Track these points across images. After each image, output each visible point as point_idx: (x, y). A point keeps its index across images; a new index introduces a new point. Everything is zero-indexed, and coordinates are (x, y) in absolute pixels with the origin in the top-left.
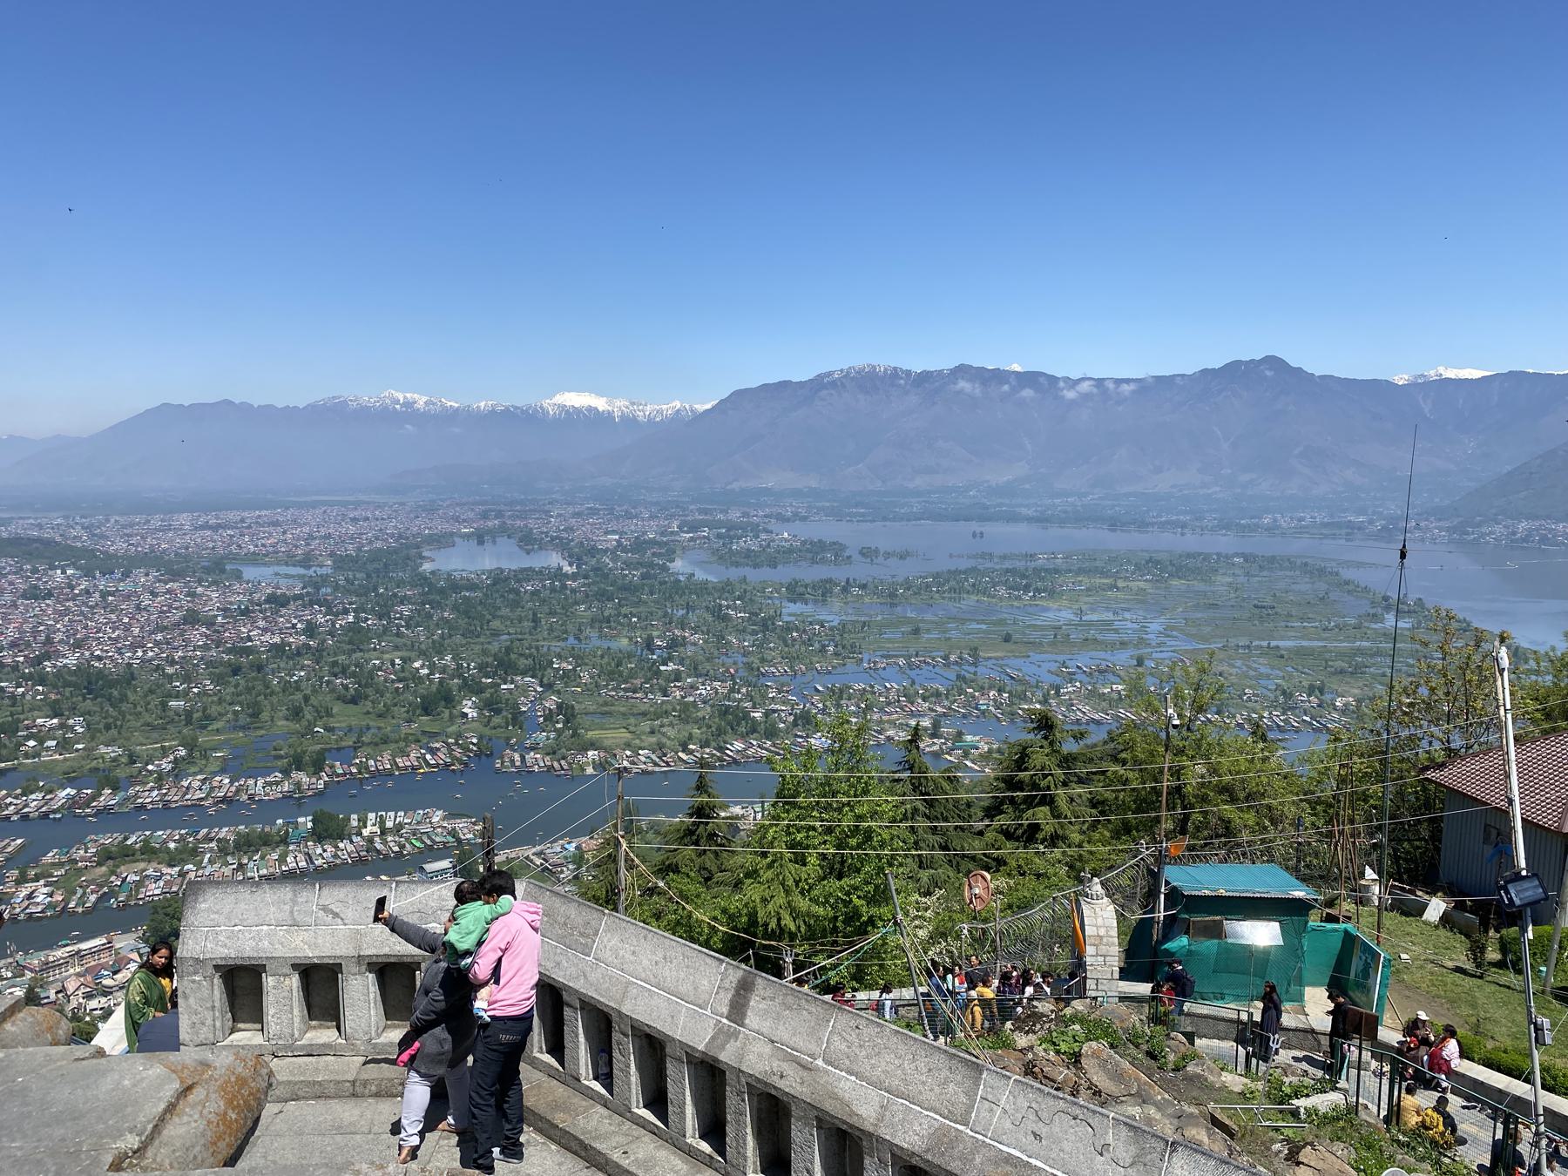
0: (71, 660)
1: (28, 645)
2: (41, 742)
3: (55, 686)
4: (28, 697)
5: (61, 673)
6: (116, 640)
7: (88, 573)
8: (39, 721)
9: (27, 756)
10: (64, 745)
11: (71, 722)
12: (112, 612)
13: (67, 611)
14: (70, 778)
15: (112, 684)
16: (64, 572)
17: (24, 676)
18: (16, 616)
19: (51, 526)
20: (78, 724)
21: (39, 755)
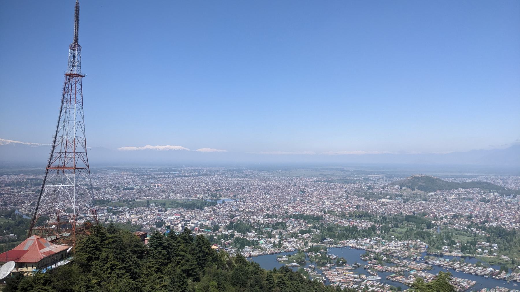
0: (494, 224)
1: (481, 217)
2: (483, 250)
3: (488, 232)
4: (480, 234)
5: (491, 228)
6: (510, 219)
7: (502, 195)
8: (483, 243)
9: (478, 253)
10: (490, 253)
11: (493, 245)
12: (509, 209)
13: (494, 207)
14: (491, 264)
15: (508, 234)
16: (494, 194)
17: (479, 227)
18: (478, 207)
19: (490, 179)
20: (495, 246)
21: (481, 254)
